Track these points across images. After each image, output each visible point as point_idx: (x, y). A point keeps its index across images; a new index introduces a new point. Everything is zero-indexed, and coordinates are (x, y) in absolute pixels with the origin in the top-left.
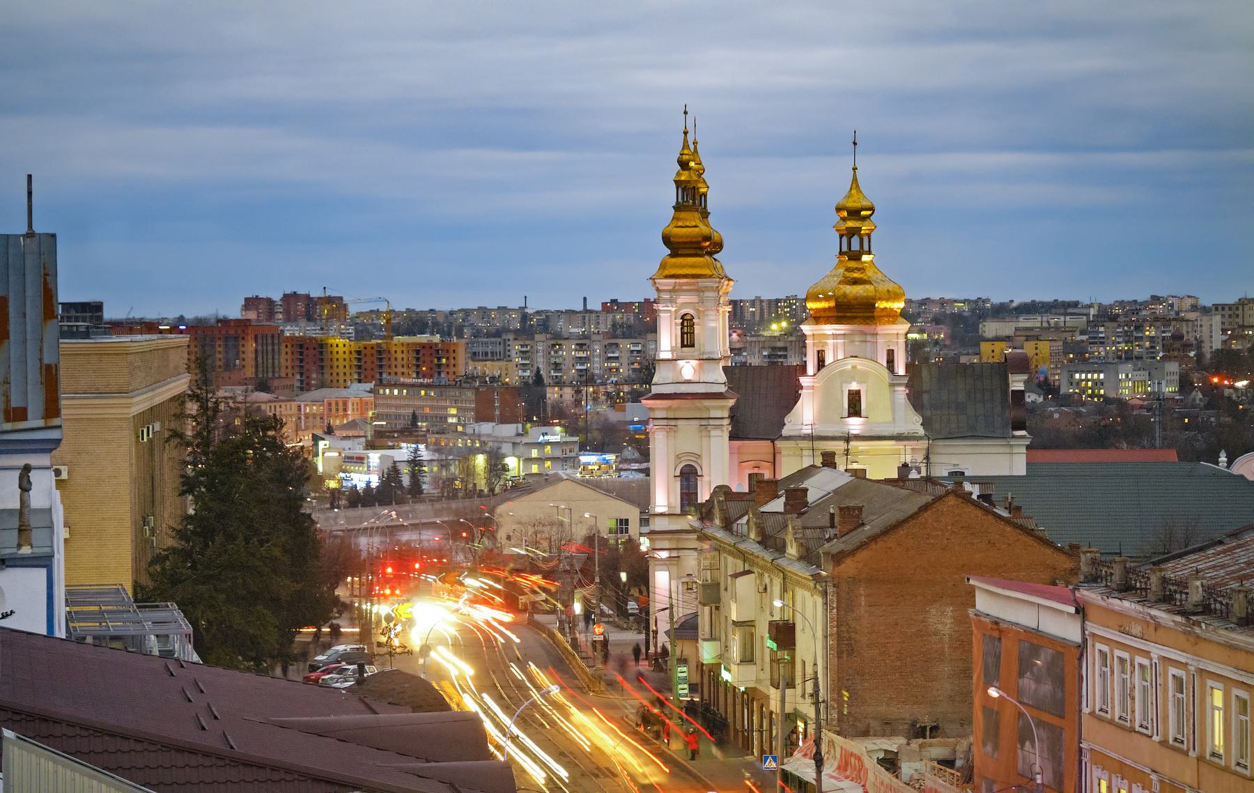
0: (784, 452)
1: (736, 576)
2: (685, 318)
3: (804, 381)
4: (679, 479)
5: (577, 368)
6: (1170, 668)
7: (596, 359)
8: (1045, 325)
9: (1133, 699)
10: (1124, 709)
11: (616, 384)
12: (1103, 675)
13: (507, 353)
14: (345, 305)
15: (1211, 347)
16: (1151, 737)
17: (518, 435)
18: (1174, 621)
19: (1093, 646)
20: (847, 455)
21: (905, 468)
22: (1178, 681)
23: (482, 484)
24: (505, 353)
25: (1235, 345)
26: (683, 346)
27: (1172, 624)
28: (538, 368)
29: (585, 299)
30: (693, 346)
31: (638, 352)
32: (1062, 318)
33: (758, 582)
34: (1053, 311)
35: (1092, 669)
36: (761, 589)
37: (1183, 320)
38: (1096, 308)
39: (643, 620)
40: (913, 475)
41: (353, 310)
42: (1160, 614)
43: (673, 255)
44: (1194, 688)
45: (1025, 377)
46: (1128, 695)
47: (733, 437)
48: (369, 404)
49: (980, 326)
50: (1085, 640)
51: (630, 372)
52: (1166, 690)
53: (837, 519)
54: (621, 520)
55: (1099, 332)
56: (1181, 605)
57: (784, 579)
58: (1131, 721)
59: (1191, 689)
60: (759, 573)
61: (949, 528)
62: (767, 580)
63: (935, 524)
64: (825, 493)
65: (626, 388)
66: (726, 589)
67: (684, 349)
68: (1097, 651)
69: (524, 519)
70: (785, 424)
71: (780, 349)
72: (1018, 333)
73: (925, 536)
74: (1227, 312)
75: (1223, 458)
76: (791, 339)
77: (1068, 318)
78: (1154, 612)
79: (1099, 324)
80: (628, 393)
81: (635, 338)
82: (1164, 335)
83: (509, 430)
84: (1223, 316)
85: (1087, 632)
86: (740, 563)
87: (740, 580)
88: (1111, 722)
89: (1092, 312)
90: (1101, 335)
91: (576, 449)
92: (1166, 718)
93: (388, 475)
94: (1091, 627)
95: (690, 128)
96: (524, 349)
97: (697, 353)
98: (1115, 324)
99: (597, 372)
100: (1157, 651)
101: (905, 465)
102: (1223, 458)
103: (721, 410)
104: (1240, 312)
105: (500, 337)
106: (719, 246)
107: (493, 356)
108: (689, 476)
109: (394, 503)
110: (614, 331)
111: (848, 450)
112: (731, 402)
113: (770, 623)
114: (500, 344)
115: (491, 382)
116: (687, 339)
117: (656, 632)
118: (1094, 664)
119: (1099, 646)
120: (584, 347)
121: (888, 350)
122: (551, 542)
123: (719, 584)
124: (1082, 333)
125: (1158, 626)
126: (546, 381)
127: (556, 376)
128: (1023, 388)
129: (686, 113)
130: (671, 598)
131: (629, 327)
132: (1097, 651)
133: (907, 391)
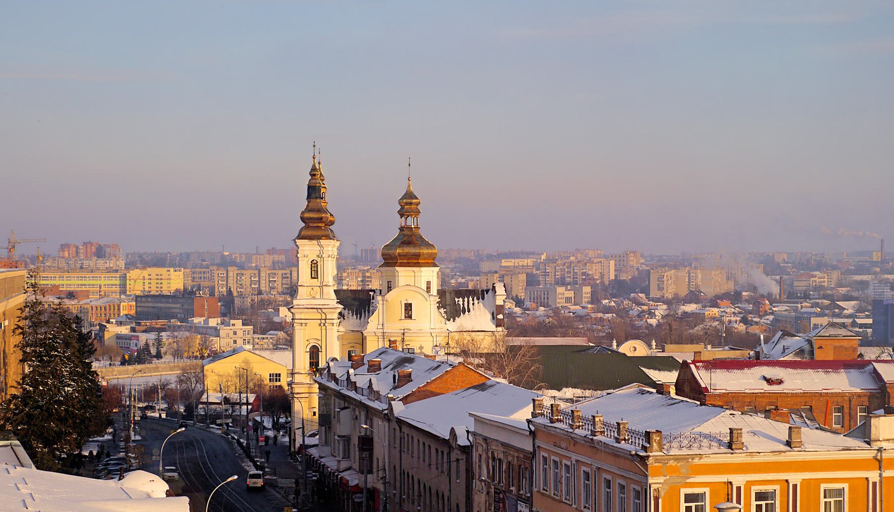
0: (368, 338)
6: (582, 467)
8: (516, 264)
9: (562, 483)
10: (556, 489)
12: (545, 470)
13: (213, 278)
15: (609, 278)
16: (571, 505)
19: (540, 453)
22: (587, 475)
24: (211, 277)
27: (584, 442)
32: (526, 261)
35: (538, 466)
38: (545, 254)
43: (307, 227)
44: (595, 478)
46: (557, 482)
50: (534, 450)
52: (579, 480)
54: (276, 374)
57: (367, 412)
58: (560, 496)
59: (594, 479)
60: (353, 408)
62: (357, 413)
63: (452, 382)
66: (334, 417)
69: (222, 373)
71: (368, 277)
72: (501, 269)
74: (618, 258)
75: (615, 344)
80: (282, 301)
83: (213, 322)
84: (616, 261)
85: (536, 446)
86: (342, 402)
87: (343, 413)
88: (549, 497)
89: (543, 257)
92: (580, 495)
94: (538, 443)
95: (317, 154)
96: (222, 276)
98: (555, 265)
100: (574, 457)
102: (615, 344)
104: (625, 259)
110: (274, 266)
111: (404, 339)
113: (359, 437)
115: (203, 294)
119: (542, 453)
126: (235, 294)
127: (240, 291)
129: (314, 146)
131: (282, 263)
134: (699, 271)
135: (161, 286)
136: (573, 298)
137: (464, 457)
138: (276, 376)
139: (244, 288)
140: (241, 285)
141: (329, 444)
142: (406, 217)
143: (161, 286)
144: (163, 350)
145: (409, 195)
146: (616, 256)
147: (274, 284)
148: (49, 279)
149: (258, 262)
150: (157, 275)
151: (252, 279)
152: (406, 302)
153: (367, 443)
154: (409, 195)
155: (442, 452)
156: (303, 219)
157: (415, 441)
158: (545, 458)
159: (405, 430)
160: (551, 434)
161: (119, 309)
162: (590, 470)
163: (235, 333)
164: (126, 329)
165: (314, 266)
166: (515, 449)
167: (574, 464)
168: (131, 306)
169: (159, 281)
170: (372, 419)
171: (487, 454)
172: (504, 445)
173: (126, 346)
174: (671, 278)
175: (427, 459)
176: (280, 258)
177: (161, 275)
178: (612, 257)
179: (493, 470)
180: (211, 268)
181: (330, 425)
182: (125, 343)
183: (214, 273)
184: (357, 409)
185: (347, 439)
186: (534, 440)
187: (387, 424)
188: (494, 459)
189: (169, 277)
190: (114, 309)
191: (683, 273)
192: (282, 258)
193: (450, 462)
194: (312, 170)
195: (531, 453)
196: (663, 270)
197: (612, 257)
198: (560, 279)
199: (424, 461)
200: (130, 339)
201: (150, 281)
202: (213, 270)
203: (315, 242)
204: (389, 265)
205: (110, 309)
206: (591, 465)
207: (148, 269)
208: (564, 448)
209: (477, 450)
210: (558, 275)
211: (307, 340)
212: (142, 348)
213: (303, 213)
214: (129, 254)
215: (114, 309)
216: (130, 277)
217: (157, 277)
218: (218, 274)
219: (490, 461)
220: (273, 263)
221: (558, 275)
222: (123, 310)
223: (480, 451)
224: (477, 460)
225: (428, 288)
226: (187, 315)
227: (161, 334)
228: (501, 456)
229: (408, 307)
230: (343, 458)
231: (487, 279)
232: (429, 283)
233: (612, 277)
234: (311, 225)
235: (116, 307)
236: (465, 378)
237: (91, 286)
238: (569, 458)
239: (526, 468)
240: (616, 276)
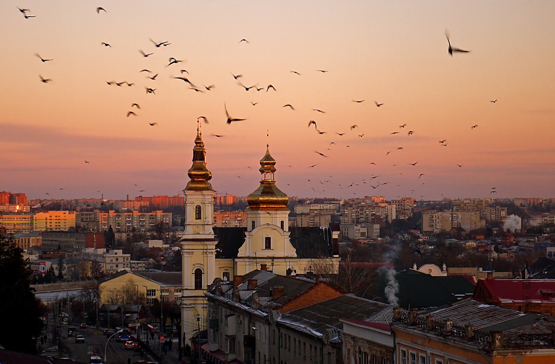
1: (227, 317)
2: (197, 207)
3: (246, 233)
4: (194, 275)
5: (127, 225)
7: (135, 221)
8: (322, 208)
14: (26, 197)
15: (392, 218)
17: (104, 253)
18: (438, 339)
19: (399, 348)
20: (273, 266)
21: (289, 271)
23: (89, 274)
25: (402, 217)
27: (437, 340)
28: (110, 225)
29: (128, 196)
30: (201, 219)
32: (329, 205)
33: (237, 319)
34: (325, 202)
36: (239, 321)
37: (380, 207)
38: (343, 200)
39: (179, 334)
40: (293, 274)
41: (28, 199)
42: (431, 335)
43: (193, 181)
45: (339, 232)
47: (217, 257)
48: (39, 240)
49: (295, 208)
51: (150, 226)
53: (272, 293)
54: (152, 290)
55: (345, 211)
56: (440, 332)
57: (250, 317)
60: (237, 315)
61: (321, 297)
62: (242, 318)
64: (265, 282)
65: (148, 234)
66: (222, 322)
67: (196, 220)
68: (401, 350)
69: (112, 289)
70: (239, 252)
73: (312, 300)
74: (397, 204)
75: (415, 267)
76: (218, 213)
77: (331, 205)
78: (428, 335)
79: (345, 208)
80: (150, 236)
81: (152, 212)
82: (372, 213)
85: (396, 343)
86: (228, 311)
89: (342, 203)
90: (346, 213)
91: (129, 259)
93: (49, 270)
96: (105, 217)
97: (202, 222)
98: (352, 208)
99: (136, 227)
101: (289, 269)
102: (415, 267)
103: (212, 246)
104: (403, 203)
105: (93, 211)
106: (210, 178)
107: (90, 219)
108: (198, 274)
109: (52, 282)
111: (273, 264)
112: (216, 243)
113: (244, 336)
114: (93, 214)
115: (92, 231)
116: (198, 217)
117: (184, 339)
118: (399, 356)
119: (402, 348)
120: (130, 216)
121: (281, 221)
122: (123, 299)
123: (218, 320)
124: (338, 212)
125: (430, 340)
126: (114, 230)
128: (337, 238)
130: (199, 325)
131: (147, 207)
132: (401, 350)
133: (290, 238)
134: (459, 212)
135: (59, 224)
136: (366, 233)
137: (335, 351)
138: (152, 292)
139: (121, 226)
140: (118, 223)
141: (217, 341)
142: (265, 173)
143: (59, 224)
144: (63, 272)
145: (268, 157)
146: (396, 202)
147: (143, 223)
148: (7, 219)
149: (129, 207)
150: (56, 216)
151: (127, 219)
152: (266, 237)
153: (250, 341)
154: (268, 157)
155: (316, 348)
156: (190, 175)
157: (292, 339)
158: (404, 352)
159: (283, 331)
160: (409, 333)
161: (29, 242)
162: (442, 361)
163: (117, 260)
164: (36, 257)
165: (199, 210)
166: (378, 345)
167: (429, 356)
168: (38, 240)
169: (58, 221)
170: (254, 323)
171: (354, 348)
172: (369, 342)
173: (36, 269)
174: (438, 218)
175: (302, 353)
176: (145, 204)
177: (59, 216)
178: (393, 202)
179: (360, 361)
180: (95, 211)
181: (218, 327)
182: (37, 267)
183: (97, 215)
184: (241, 316)
185: (233, 339)
186: (394, 339)
187: (267, 327)
188: (360, 352)
189: (65, 218)
190: (25, 242)
191: (447, 214)
192: (147, 204)
193: (323, 355)
194: (196, 139)
195: (392, 348)
196: (433, 212)
197: (393, 202)
198: (355, 219)
199: (300, 354)
200: (39, 264)
201: (51, 221)
202: (97, 213)
203: (199, 193)
204: (253, 209)
205: (22, 242)
206: (444, 357)
207: (49, 212)
208: (421, 344)
209: (346, 346)
210: (353, 216)
211: (194, 265)
212: (48, 271)
214: (32, 200)
215: (25, 242)
216: (36, 218)
217: (56, 218)
218: (102, 216)
219: (357, 354)
220: (141, 207)
221: (353, 216)
222: (32, 242)
223: (349, 346)
224: (346, 354)
225: (282, 227)
226: (81, 247)
227: (62, 261)
228: (367, 351)
229: (268, 240)
230: (230, 352)
231: (302, 219)
232: (282, 222)
233: (394, 217)
234: (195, 179)
235: (27, 241)
236: (325, 293)
237: (7, 225)
238: (425, 352)
239: (388, 359)
240: (397, 216)
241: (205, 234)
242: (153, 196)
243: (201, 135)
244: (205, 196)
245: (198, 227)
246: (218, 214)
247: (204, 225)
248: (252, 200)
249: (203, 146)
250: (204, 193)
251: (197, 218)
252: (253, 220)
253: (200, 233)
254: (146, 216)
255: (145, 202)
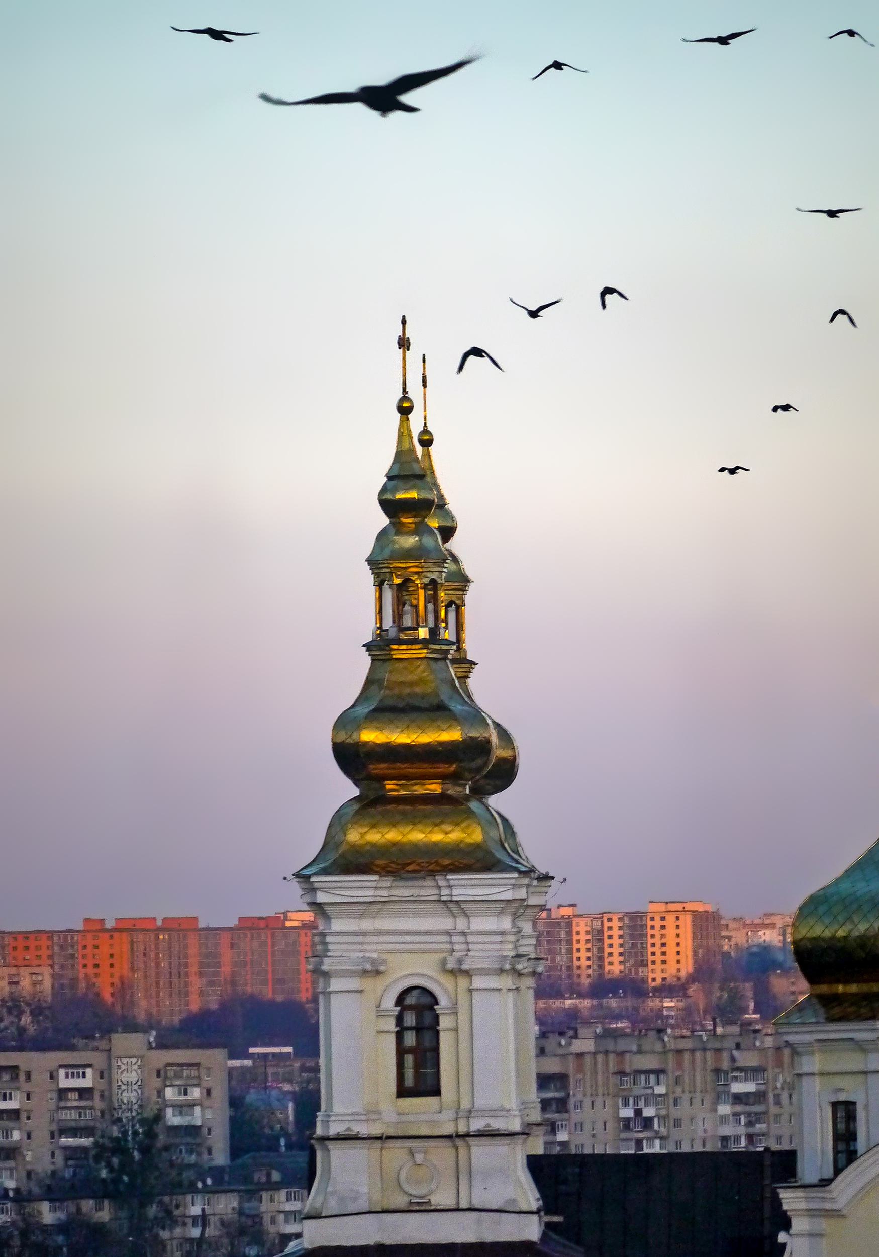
2: (410, 1000)
11: (20, 1198)
26: (402, 1092)
31: (84, 1093)
51: (59, 1159)
81: (72, 1048)
95: (415, 391)
97: (448, 1115)
129: (404, 343)
194: (390, 478)
203: (426, 889)
204: (836, 1011)
213: (344, 722)
241: (470, 1210)
242: (80, 926)
243: (426, 442)
244: (468, 916)
245: (419, 1158)
246: (580, 1055)
247: (459, 1142)
248: (833, 938)
249: (448, 532)
250: (459, 893)
251: (409, 1081)
252: (842, 1097)
253: (442, 1199)
254: (28, 1076)
255: (25, 972)
